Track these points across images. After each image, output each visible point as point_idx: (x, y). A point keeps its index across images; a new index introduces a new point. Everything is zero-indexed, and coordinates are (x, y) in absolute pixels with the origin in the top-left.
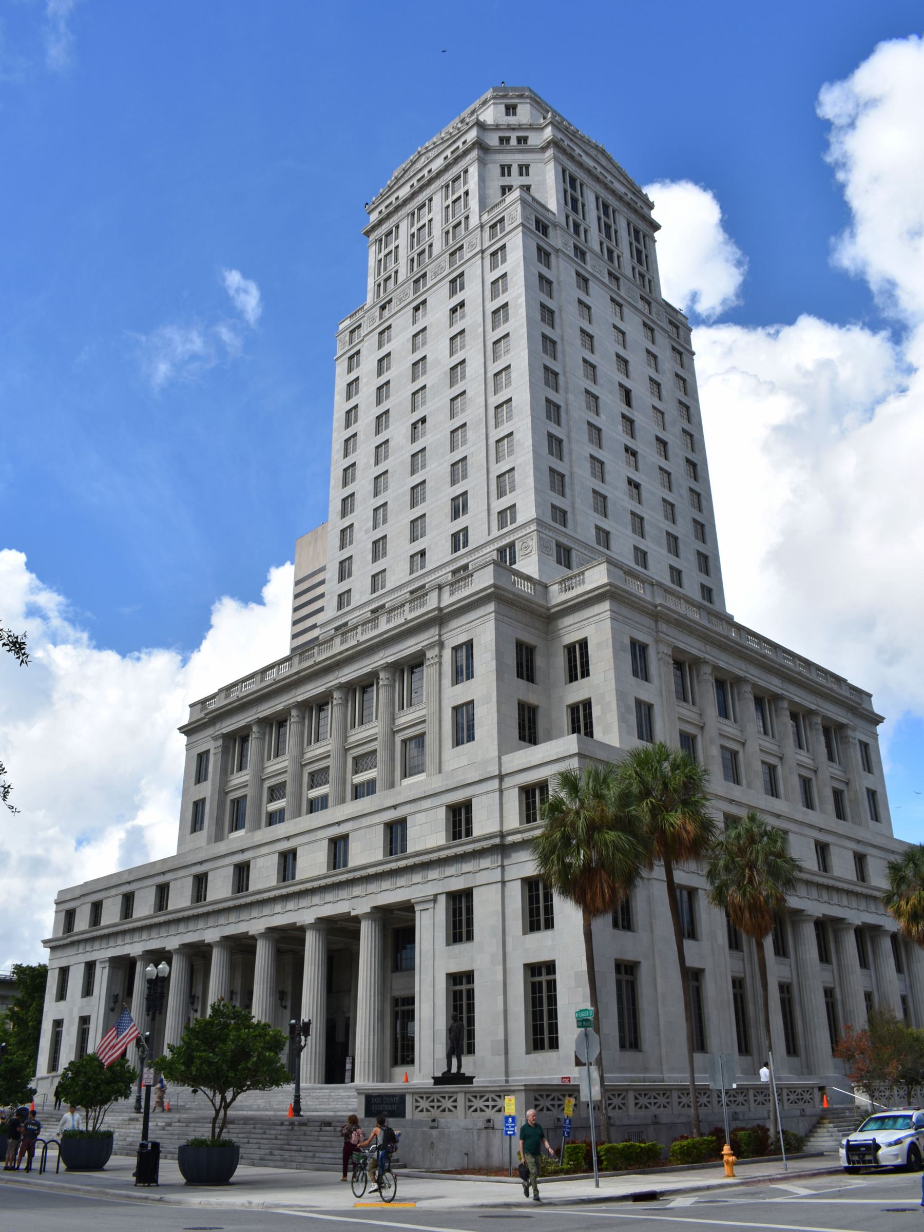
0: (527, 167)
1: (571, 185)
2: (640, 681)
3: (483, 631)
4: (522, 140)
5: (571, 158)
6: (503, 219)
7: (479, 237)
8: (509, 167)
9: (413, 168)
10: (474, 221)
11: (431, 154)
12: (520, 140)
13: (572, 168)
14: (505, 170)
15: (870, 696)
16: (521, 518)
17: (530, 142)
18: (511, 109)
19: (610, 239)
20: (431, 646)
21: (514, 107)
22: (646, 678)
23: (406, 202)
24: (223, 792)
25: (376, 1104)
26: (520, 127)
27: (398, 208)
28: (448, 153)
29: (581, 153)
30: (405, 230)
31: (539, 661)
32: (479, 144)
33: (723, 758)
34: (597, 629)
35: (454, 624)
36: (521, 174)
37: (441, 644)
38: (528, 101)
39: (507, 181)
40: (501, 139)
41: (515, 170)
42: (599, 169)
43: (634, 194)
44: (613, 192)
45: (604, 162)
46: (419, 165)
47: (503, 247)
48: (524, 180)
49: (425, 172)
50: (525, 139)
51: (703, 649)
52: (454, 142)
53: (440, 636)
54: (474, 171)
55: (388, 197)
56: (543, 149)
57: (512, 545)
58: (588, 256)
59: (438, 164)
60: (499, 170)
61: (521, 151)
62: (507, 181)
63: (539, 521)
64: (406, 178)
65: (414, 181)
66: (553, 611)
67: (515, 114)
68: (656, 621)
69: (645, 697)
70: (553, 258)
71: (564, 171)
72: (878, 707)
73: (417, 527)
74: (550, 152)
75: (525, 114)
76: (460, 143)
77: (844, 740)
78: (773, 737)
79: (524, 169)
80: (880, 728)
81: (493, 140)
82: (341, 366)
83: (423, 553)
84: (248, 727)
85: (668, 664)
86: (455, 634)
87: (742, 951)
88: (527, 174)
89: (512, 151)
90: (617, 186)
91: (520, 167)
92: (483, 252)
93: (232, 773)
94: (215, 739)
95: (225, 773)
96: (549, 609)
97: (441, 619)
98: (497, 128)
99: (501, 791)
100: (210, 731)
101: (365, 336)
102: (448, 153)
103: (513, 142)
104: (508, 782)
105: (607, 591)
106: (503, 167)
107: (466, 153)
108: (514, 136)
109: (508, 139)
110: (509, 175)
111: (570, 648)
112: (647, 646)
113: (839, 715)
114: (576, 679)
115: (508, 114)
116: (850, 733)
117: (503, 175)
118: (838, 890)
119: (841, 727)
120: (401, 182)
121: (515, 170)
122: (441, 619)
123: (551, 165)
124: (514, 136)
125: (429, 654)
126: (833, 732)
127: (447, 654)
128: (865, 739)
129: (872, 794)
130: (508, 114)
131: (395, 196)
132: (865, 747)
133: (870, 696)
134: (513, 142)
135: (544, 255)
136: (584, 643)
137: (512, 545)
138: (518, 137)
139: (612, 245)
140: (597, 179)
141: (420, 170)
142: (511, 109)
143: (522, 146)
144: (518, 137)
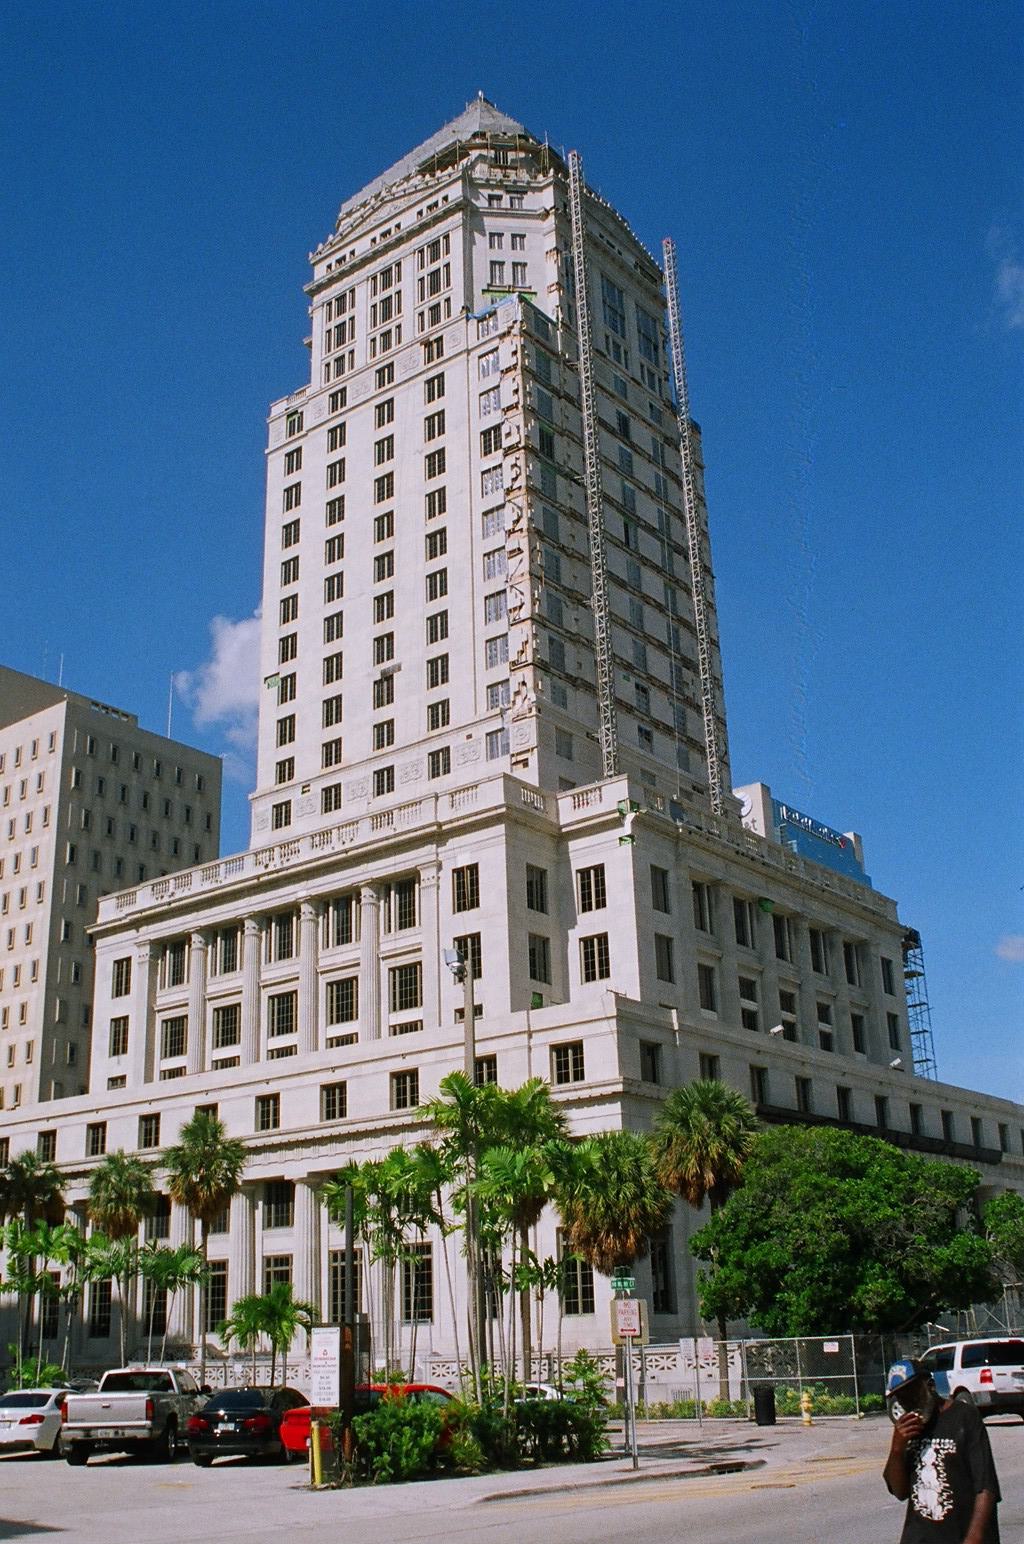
0: (523, 237)
3: (490, 853)
9: (373, 217)
11: (402, 203)
15: (896, 904)
22: (666, 910)
23: (365, 261)
24: (151, 1013)
32: (464, 206)
33: (797, 1085)
35: (452, 843)
36: (514, 247)
39: (496, 255)
40: (491, 198)
41: (507, 240)
46: (383, 213)
48: (519, 256)
49: (391, 225)
54: (457, 240)
55: (340, 249)
59: (409, 220)
64: (366, 227)
65: (377, 234)
66: (564, 830)
69: (664, 932)
76: (439, 197)
77: (865, 957)
79: (518, 238)
82: (276, 464)
86: (459, 853)
91: (514, 236)
92: (468, 351)
96: (561, 828)
97: (439, 836)
99: (530, 1048)
101: (308, 431)
102: (424, 206)
104: (537, 1039)
110: (500, 246)
113: (857, 929)
116: (873, 950)
119: (863, 945)
121: (507, 240)
122: (439, 836)
125: (423, 875)
126: (854, 951)
129: (893, 1019)
133: (896, 904)
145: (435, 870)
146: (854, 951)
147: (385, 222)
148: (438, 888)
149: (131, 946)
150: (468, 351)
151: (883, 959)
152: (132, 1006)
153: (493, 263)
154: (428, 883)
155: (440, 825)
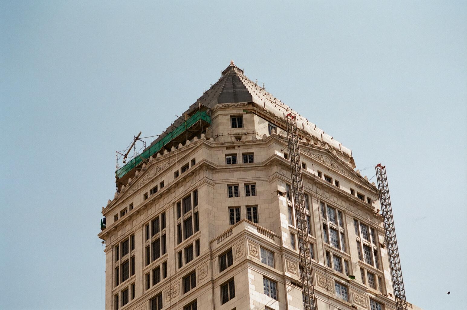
0: (253, 187)
4: (248, 158)
7: (209, 265)
14: (233, 191)
28: (178, 168)
36: (248, 194)
41: (242, 189)
48: (251, 201)
50: (251, 155)
60: (226, 191)
70: (280, 285)
79: (251, 189)
88: (254, 194)
91: (247, 186)
103: (240, 160)
106: (230, 188)
109: (234, 156)
110: (237, 195)
117: (231, 196)
121: (242, 189)
124: (239, 152)
130: (234, 126)
134: (240, 160)
143: (249, 165)
147: (153, 181)
153: (231, 209)
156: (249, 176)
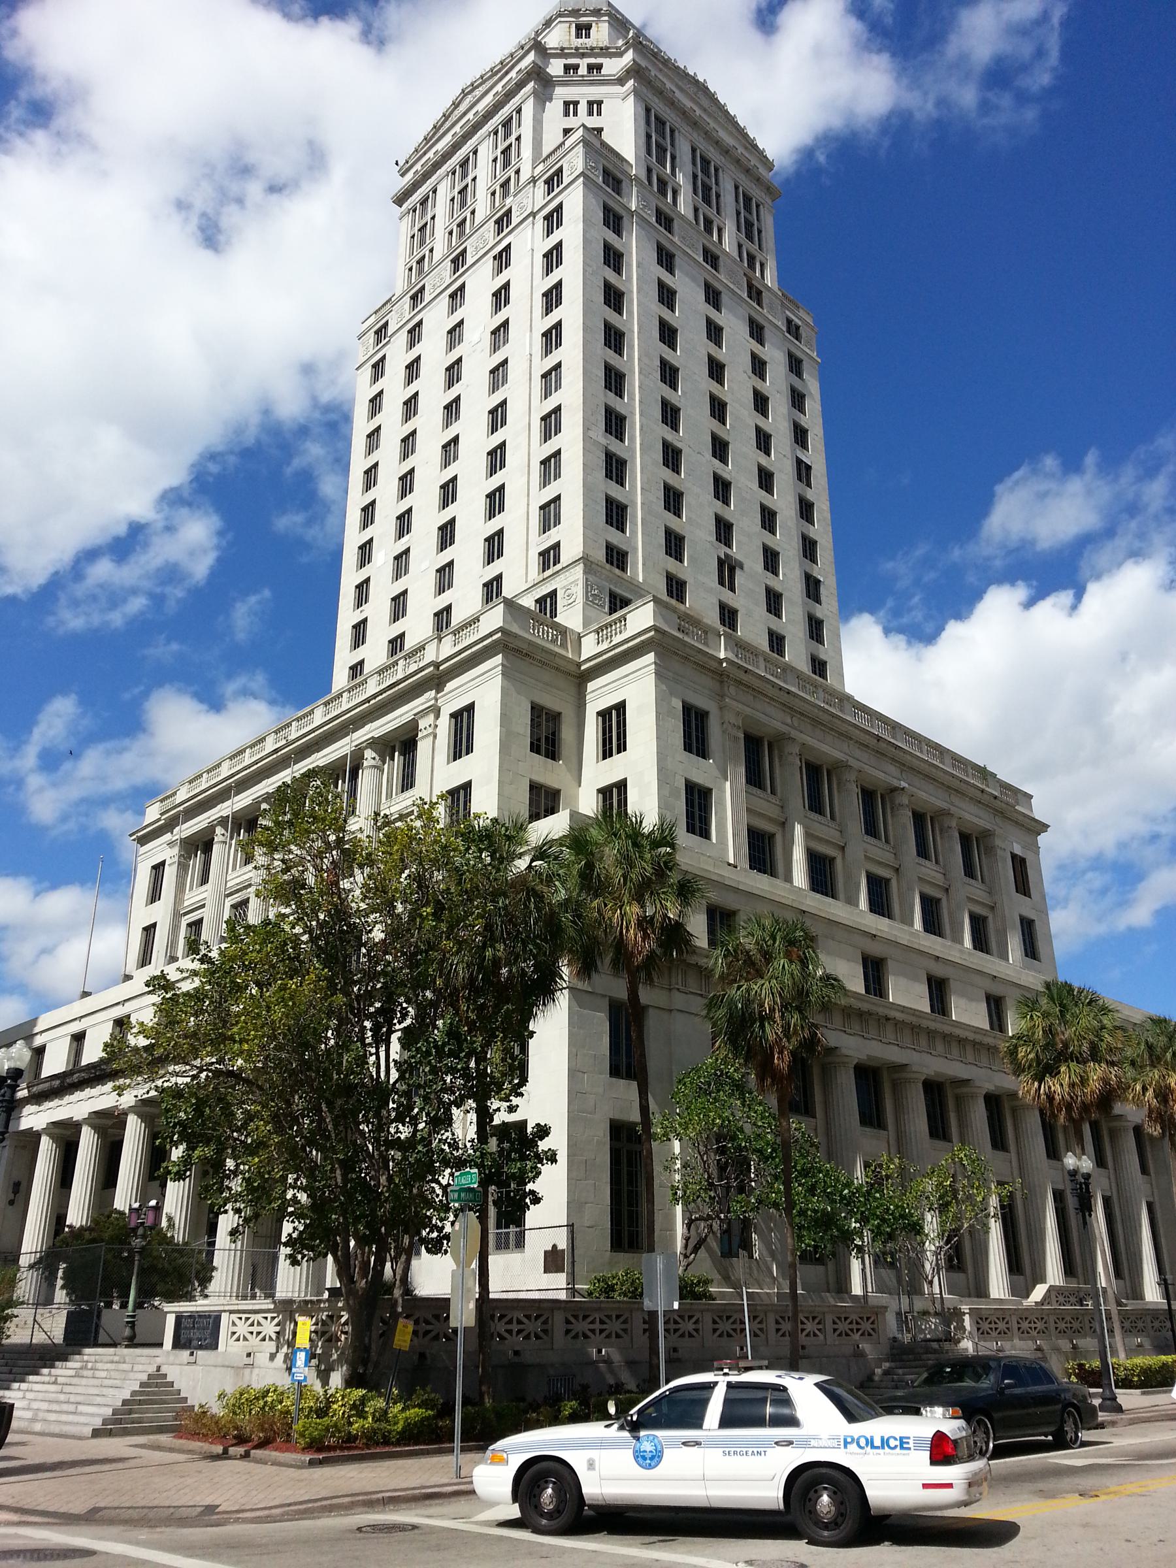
0: (599, 103)
1: (657, 132)
2: (693, 757)
3: (485, 690)
4: (595, 68)
5: (660, 93)
6: (560, 170)
7: (531, 195)
8: (576, 103)
9: (456, 112)
10: (525, 175)
12: (591, 68)
13: (659, 107)
14: (570, 107)
16: (565, 559)
17: (603, 72)
18: (583, 30)
19: (708, 203)
20: (423, 713)
21: (588, 27)
25: (186, 1328)
26: (591, 52)
27: (437, 166)
29: (674, 89)
30: (445, 192)
31: (567, 734)
34: (637, 688)
36: (590, 113)
37: (437, 712)
38: (606, 18)
39: (571, 122)
40: (567, 68)
41: (583, 108)
42: (698, 112)
43: (746, 148)
44: (717, 143)
45: (705, 102)
47: (560, 207)
48: (593, 122)
50: (599, 67)
51: (789, 721)
52: (507, 73)
53: (437, 700)
55: (425, 153)
56: (621, 81)
57: (553, 594)
58: (676, 225)
61: (592, 83)
62: (571, 122)
63: (586, 560)
65: (457, 128)
67: (588, 36)
68: (722, 682)
69: (699, 778)
71: (648, 110)
72: (1039, 810)
73: (445, 575)
74: (630, 83)
75: (601, 34)
77: (990, 850)
78: (887, 841)
79: (595, 106)
80: (1042, 839)
81: (555, 68)
83: (448, 609)
84: (210, 830)
85: (736, 738)
86: (453, 697)
87: (814, 1117)
88: (599, 114)
89: (583, 82)
90: (722, 135)
91: (590, 104)
93: (191, 889)
94: (171, 844)
95: (180, 888)
96: (579, 665)
97: (437, 679)
98: (562, 53)
100: (167, 837)
102: (499, 88)
103: (583, 70)
105: (652, 638)
107: (520, 85)
108: (583, 63)
110: (575, 114)
111: (604, 714)
112: (707, 713)
114: (611, 755)
115: (578, 36)
117: (567, 114)
118: (962, 1042)
119: (985, 836)
120: (441, 131)
121: (583, 108)
123: (631, 98)
125: (422, 724)
126: (973, 844)
127: (444, 723)
128: (1018, 850)
131: (434, 150)
132: (1019, 864)
134: (583, 70)
135: (614, 220)
136: (621, 707)
137: (553, 594)
138: (588, 65)
139: (712, 213)
140: (695, 124)
141: (465, 114)
142: (583, 30)
144: (588, 65)
145: (432, 716)
146: (973, 844)
148: (435, 737)
149: (164, 850)
150: (533, 214)
151: (1014, 856)
152: (161, 913)
154: (425, 733)
155: (437, 665)
156: (594, 92)
